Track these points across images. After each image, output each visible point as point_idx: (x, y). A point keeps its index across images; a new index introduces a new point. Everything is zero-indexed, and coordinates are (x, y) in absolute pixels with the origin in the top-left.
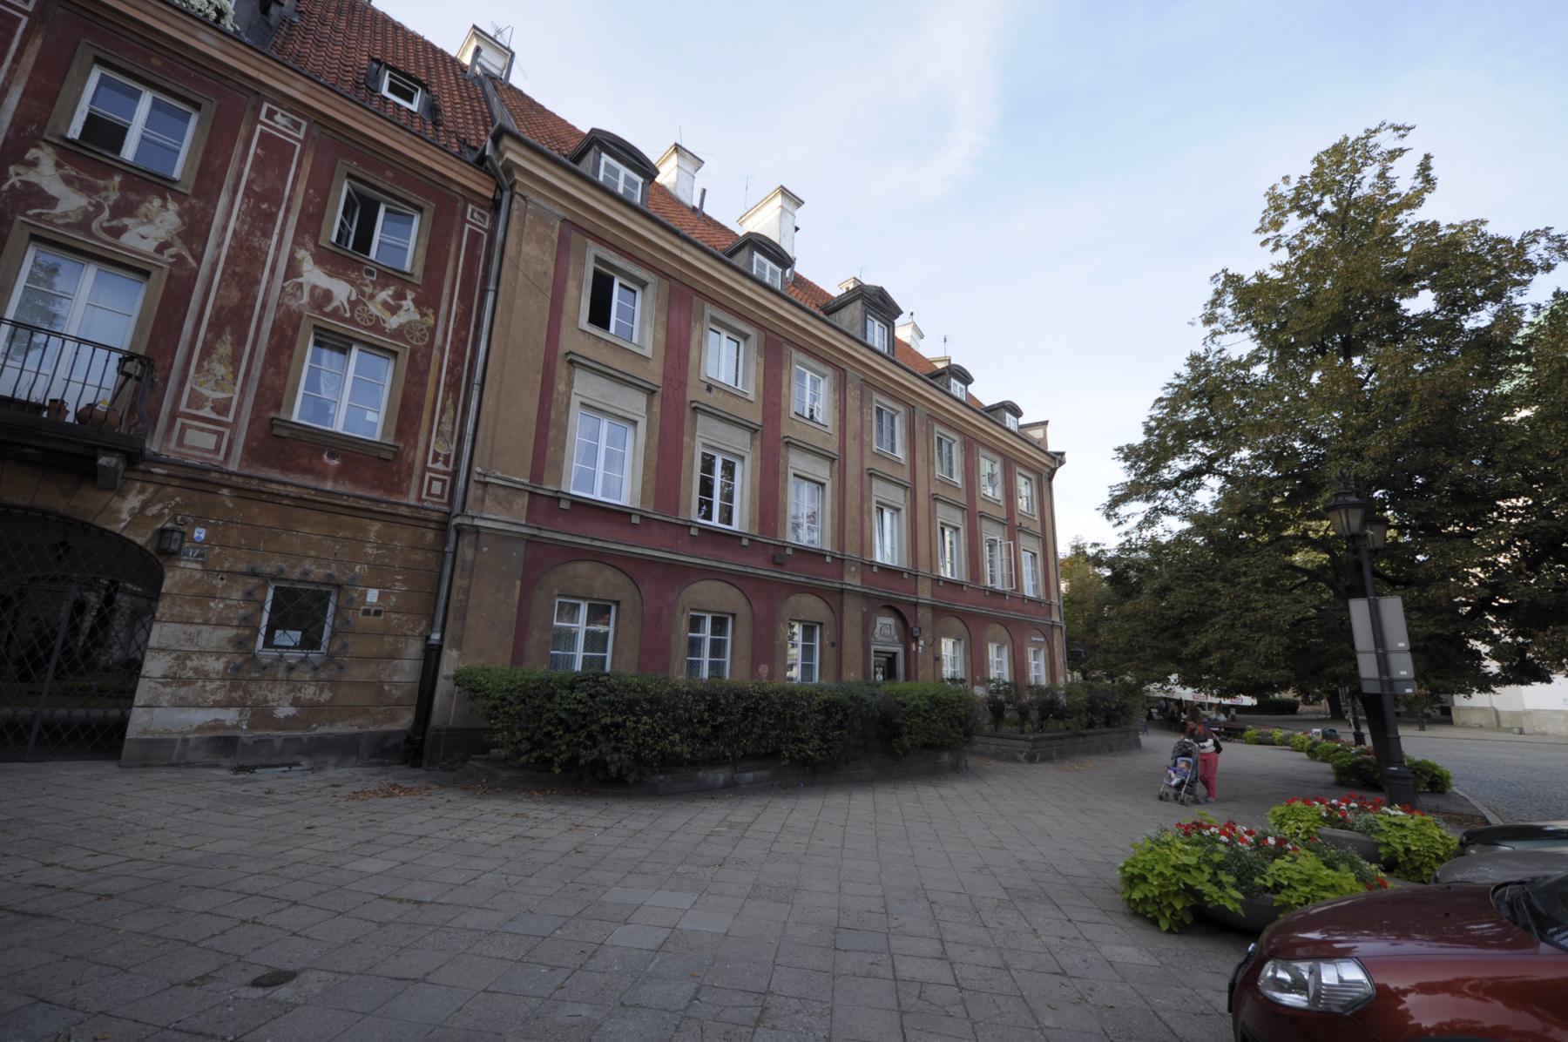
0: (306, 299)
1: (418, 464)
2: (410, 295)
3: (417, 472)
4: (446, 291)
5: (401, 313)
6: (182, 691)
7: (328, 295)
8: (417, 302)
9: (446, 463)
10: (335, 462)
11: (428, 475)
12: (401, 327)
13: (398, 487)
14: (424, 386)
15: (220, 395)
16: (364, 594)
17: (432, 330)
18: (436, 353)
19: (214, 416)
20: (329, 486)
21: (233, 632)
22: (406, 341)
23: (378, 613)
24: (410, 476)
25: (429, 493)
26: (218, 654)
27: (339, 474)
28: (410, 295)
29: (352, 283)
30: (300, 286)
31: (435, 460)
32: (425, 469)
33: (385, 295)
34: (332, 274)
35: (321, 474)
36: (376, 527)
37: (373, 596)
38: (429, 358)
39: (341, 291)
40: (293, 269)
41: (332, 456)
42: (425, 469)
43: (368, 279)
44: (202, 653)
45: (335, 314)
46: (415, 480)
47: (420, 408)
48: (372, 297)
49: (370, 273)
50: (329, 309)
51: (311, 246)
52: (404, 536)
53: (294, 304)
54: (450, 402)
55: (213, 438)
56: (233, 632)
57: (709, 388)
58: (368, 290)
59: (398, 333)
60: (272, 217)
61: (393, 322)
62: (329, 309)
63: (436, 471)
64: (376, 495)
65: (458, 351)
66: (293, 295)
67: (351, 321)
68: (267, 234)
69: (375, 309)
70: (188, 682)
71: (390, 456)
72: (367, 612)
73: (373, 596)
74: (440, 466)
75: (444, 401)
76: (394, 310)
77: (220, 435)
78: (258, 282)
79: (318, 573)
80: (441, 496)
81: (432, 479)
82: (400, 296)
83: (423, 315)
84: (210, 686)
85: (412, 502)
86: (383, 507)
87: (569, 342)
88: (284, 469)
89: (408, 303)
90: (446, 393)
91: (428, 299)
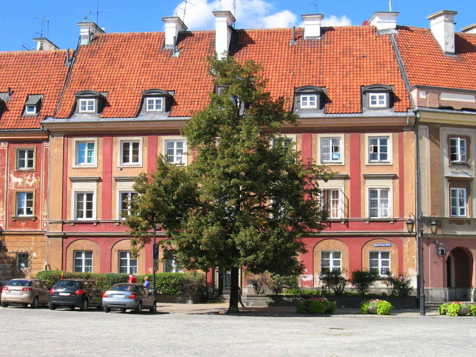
0: (14, 186)
1: (41, 220)
2: (34, 175)
3: (40, 222)
4: (42, 170)
5: (33, 181)
6: (5, 277)
7: (17, 183)
8: (36, 176)
9: (46, 218)
10: (24, 224)
11: (43, 222)
12: (33, 184)
13: (37, 227)
14: (39, 198)
15: (2, 215)
16: (33, 254)
17: (40, 182)
18: (41, 188)
19: (2, 219)
20: (24, 230)
21: (11, 264)
22: (35, 188)
23: (36, 258)
24: (39, 223)
25: (43, 227)
26: (10, 269)
27: (26, 226)
28: (34, 175)
29: (21, 178)
30: (12, 183)
31: (44, 218)
32: (42, 220)
33: (28, 178)
34: (18, 177)
35: (21, 227)
36: (33, 238)
37: (35, 254)
38: (40, 190)
39: (20, 180)
40: (10, 180)
41: (23, 222)
42: (42, 220)
43: (25, 175)
44: (7, 269)
45: (20, 187)
46: (40, 224)
47: (39, 204)
48: (26, 179)
49: (25, 173)
50: (18, 187)
51: (13, 172)
52: (40, 238)
53: (11, 188)
54: (45, 201)
55: (2, 224)
56: (11, 264)
57: (121, 169)
58: (25, 178)
59: (33, 187)
60: (4, 169)
61: (31, 184)
62: (18, 187)
63: (44, 221)
64: (33, 230)
65: (46, 186)
66: (11, 186)
67: (23, 188)
68: (4, 174)
69: (27, 182)
70: (6, 275)
71: (34, 219)
72: (34, 258)
73: (35, 254)
74: (45, 219)
75: (44, 201)
76: (30, 181)
77: (3, 223)
78: (4, 186)
79: (24, 251)
80: (46, 227)
81: (44, 223)
82: (32, 176)
83: (37, 179)
84: (9, 276)
85: (40, 230)
86: (33, 233)
87: (71, 174)
88: (15, 227)
89: (34, 177)
90: (44, 198)
91: (38, 175)
